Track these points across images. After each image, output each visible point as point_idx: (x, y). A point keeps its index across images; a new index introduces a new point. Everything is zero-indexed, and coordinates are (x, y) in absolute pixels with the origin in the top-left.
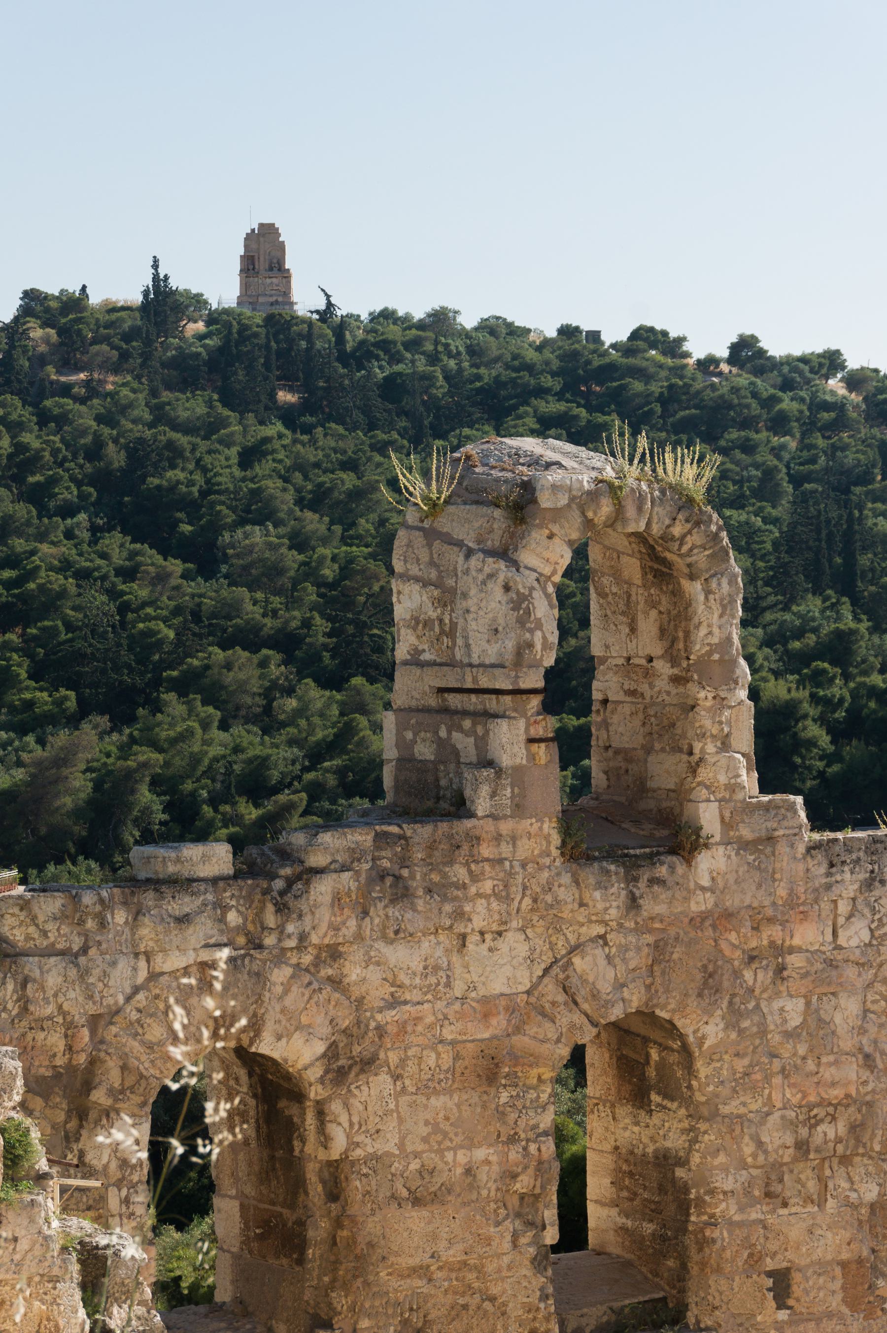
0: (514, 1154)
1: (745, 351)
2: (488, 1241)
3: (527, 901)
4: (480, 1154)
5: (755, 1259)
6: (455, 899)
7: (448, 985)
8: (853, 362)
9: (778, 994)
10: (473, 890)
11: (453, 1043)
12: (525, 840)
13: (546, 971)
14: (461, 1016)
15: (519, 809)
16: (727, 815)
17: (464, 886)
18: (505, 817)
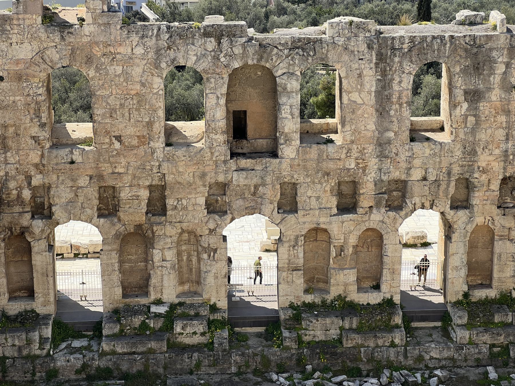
0: (29, 99)
2: (21, 120)
3: (29, 36)
4: (18, 98)
5: (107, 133)
6: (6, 34)
7: (6, 55)
9: (113, 65)
10: (12, 32)
11: (7, 70)
12: (27, 20)
13: (37, 54)
14: (10, 63)
15: (25, 12)
16: (94, 16)
17: (9, 31)
18: (21, 14)
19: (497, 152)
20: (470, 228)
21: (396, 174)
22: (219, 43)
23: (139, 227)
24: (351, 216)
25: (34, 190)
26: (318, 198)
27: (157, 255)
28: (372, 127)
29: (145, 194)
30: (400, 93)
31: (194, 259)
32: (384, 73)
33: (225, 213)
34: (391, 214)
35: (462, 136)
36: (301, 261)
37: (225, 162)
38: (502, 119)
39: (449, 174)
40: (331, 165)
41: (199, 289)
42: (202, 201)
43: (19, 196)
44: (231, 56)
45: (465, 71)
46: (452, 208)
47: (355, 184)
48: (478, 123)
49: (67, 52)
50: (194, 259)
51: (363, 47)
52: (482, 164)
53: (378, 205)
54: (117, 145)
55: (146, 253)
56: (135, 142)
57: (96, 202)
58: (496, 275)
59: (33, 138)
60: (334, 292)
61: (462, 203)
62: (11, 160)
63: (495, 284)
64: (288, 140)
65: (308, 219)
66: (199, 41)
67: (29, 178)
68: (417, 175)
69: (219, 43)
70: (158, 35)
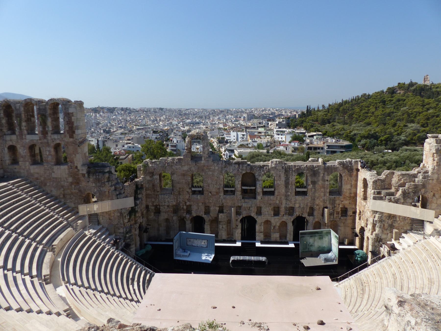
5: (207, 191)
15: (186, 157)
20: (314, 222)
21: (291, 205)
24: (277, 217)
25: (187, 206)
26: (268, 211)
27: (221, 227)
28: (284, 191)
29: (218, 209)
30: (292, 181)
32: (287, 175)
34: (290, 217)
35: (311, 194)
36: (262, 230)
37: (241, 200)
38: (323, 190)
39: (307, 206)
40: (271, 202)
43: (183, 208)
44: (242, 170)
45: (311, 175)
46: (308, 216)
47: (278, 208)
51: (281, 168)
52: (317, 203)
53: (286, 214)
54: (210, 194)
55: (218, 225)
56: (215, 194)
57: (204, 210)
59: (187, 192)
61: (311, 214)
62: (181, 198)
64: (259, 194)
66: (233, 165)
67: (186, 203)
68: (297, 206)
70: (222, 164)
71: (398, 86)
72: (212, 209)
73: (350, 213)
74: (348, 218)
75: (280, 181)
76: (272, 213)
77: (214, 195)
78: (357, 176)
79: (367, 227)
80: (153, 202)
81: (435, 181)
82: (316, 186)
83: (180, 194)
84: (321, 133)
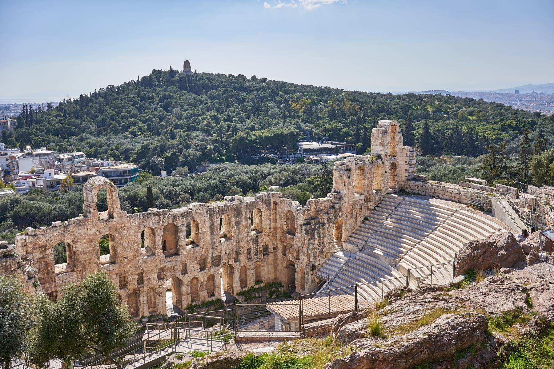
1: (254, 78)
5: (123, 256)
8: (268, 80)
15: (93, 216)
19: (245, 241)
20: (240, 267)
21: (217, 254)
22: (160, 217)
23: (134, 290)
24: (205, 271)
27: (141, 299)
28: (209, 239)
29: (136, 277)
31: (153, 299)
32: (212, 220)
33: (164, 278)
34: (217, 268)
37: (163, 260)
38: (246, 229)
40: (198, 254)
41: (155, 310)
42: (156, 276)
44: (164, 221)
45: (234, 216)
48: (239, 232)
49: (108, 229)
50: (153, 299)
53: (212, 265)
54: (126, 260)
56: (132, 258)
58: (248, 282)
60: (201, 299)
61: (237, 260)
62: (88, 273)
63: (248, 285)
65: (191, 275)
66: (153, 218)
68: (223, 253)
69: (160, 217)
71: (153, 73)
72: (129, 279)
73: (271, 249)
74: (270, 255)
75: (205, 227)
76: (199, 267)
77: (131, 260)
78: (275, 209)
79: (299, 259)
80: (48, 289)
81: (347, 204)
82: (240, 226)
83: (85, 269)
84: (81, 153)
